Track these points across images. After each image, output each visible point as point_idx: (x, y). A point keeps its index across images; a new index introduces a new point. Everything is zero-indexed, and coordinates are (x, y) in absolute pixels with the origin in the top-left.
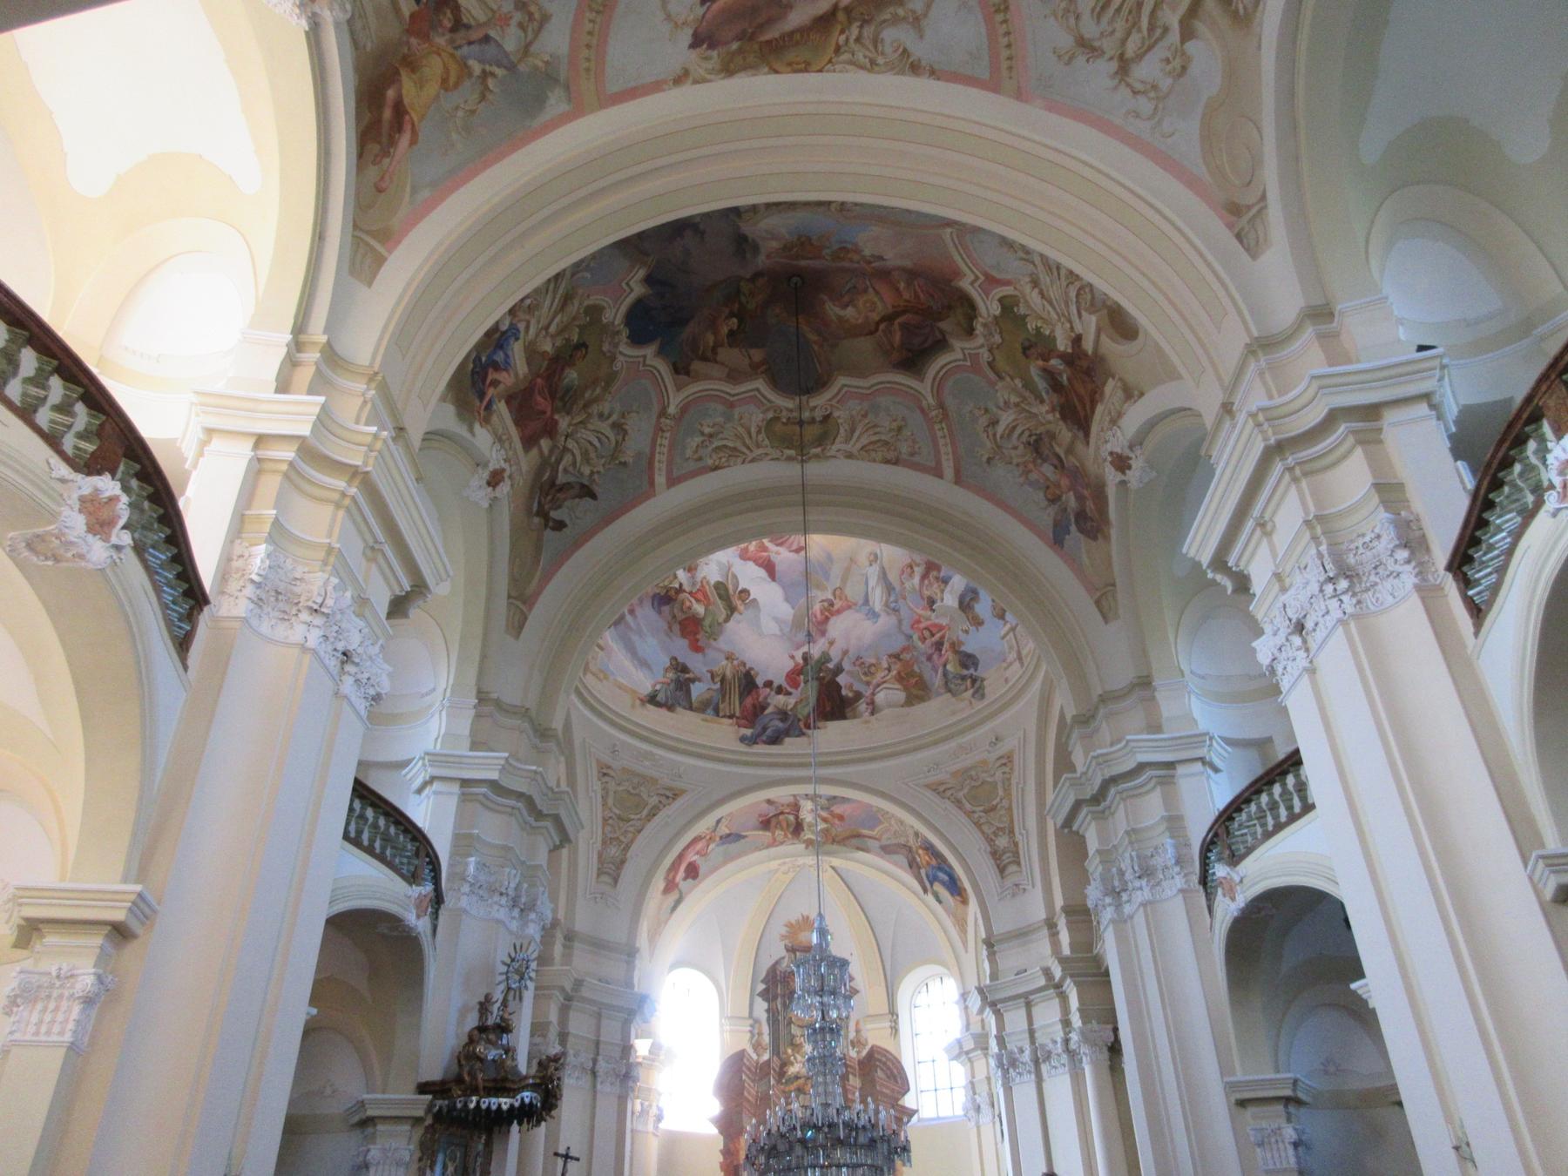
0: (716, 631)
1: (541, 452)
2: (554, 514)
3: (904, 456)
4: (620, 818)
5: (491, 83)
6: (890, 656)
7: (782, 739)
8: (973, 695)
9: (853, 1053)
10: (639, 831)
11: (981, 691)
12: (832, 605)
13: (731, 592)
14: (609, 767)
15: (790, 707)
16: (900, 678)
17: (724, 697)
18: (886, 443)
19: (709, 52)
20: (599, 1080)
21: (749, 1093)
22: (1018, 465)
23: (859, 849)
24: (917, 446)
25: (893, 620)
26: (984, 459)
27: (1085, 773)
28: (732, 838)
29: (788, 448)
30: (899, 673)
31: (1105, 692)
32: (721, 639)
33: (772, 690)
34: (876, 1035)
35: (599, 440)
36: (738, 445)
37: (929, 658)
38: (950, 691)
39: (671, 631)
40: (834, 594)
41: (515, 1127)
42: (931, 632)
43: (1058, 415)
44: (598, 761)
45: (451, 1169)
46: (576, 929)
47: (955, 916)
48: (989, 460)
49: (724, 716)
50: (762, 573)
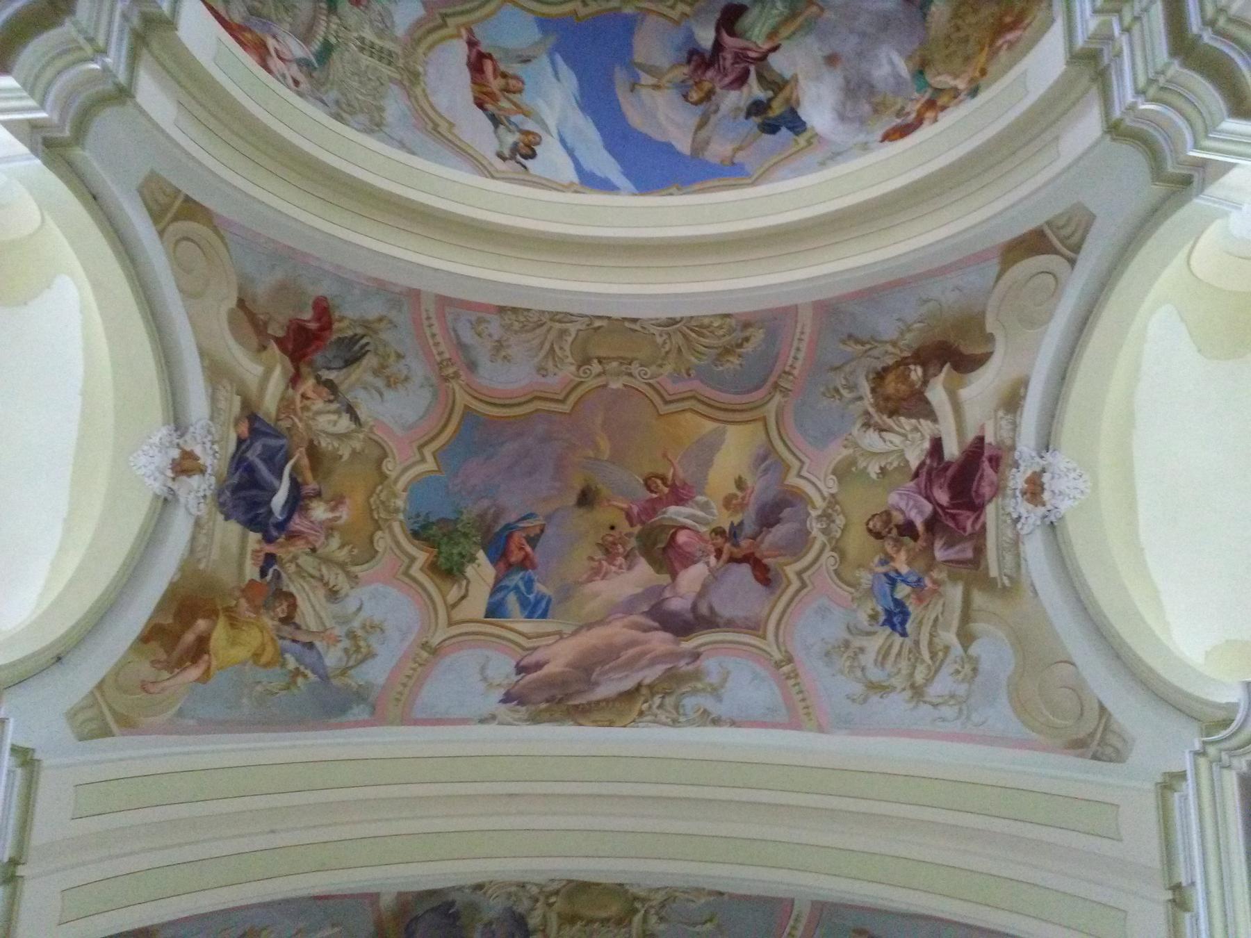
5: (300, 680)
19: (519, 707)
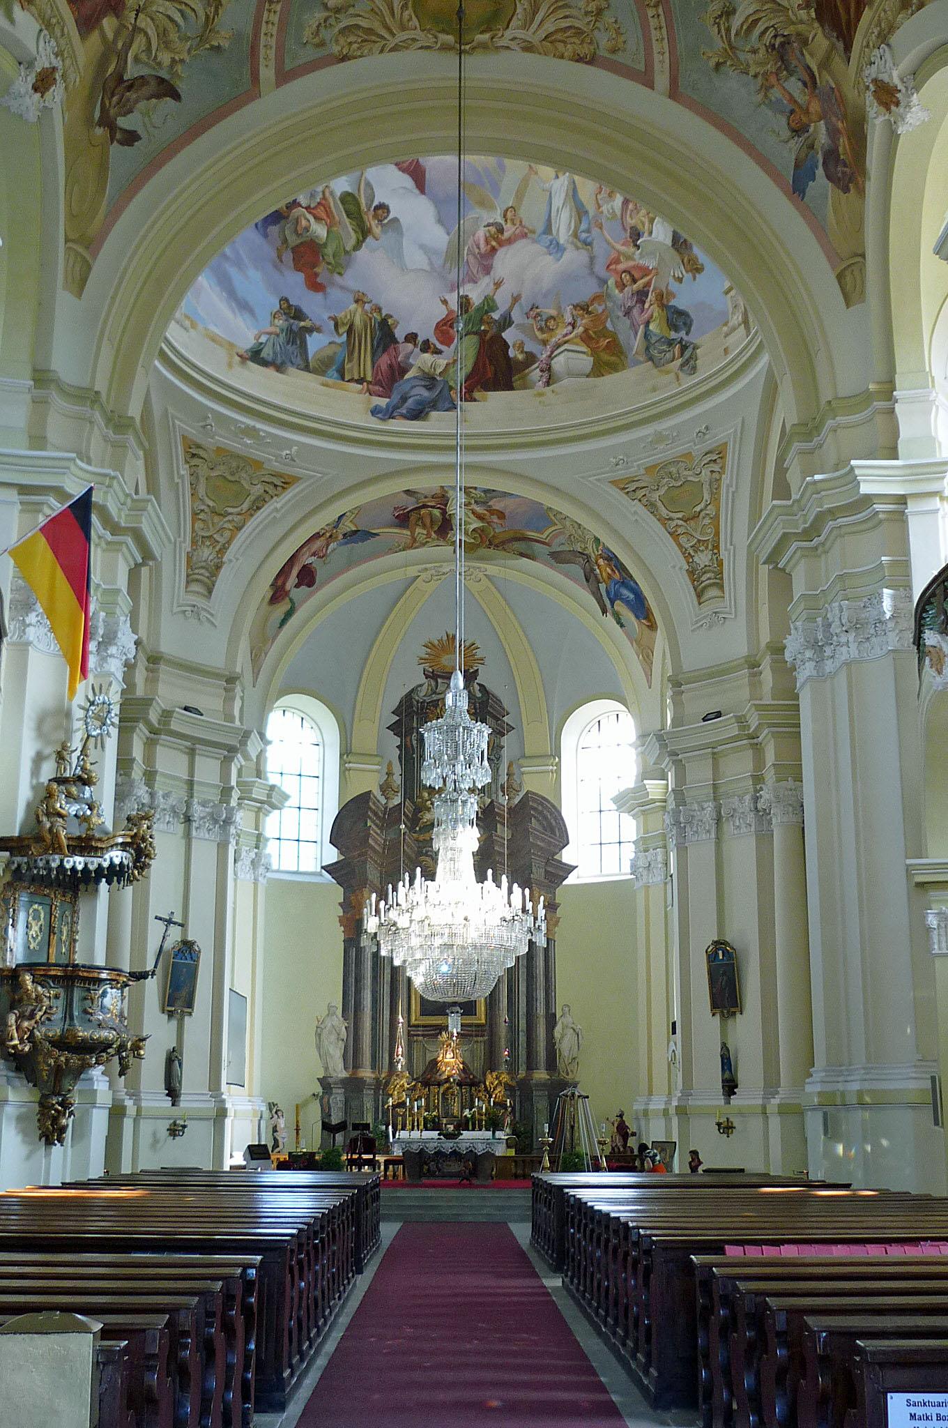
0: (341, 264)
1: (103, 36)
2: (122, 122)
3: (603, 53)
4: (214, 512)
6: (575, 307)
7: (427, 413)
8: (682, 365)
9: (504, 800)
10: (239, 529)
11: (692, 362)
12: (501, 230)
13: (364, 207)
14: (199, 446)
15: (438, 371)
16: (586, 338)
17: (351, 353)
18: (579, 32)
20: (195, 825)
21: (376, 841)
22: (755, 76)
23: (522, 555)
24: (622, 39)
25: (582, 256)
26: (712, 63)
27: (798, 501)
28: (356, 536)
29: (443, 31)
30: (586, 331)
31: (837, 398)
32: (349, 273)
33: (415, 345)
34: (531, 783)
35: (180, 11)
36: (377, 26)
37: (628, 313)
38: (651, 359)
39: (281, 261)
40: (505, 216)
41: (103, 885)
42: (632, 276)
43: (813, 15)
44: (184, 437)
45: (35, 928)
46: (162, 649)
47: (638, 643)
48: (718, 65)
49: (348, 381)
50: (407, 181)
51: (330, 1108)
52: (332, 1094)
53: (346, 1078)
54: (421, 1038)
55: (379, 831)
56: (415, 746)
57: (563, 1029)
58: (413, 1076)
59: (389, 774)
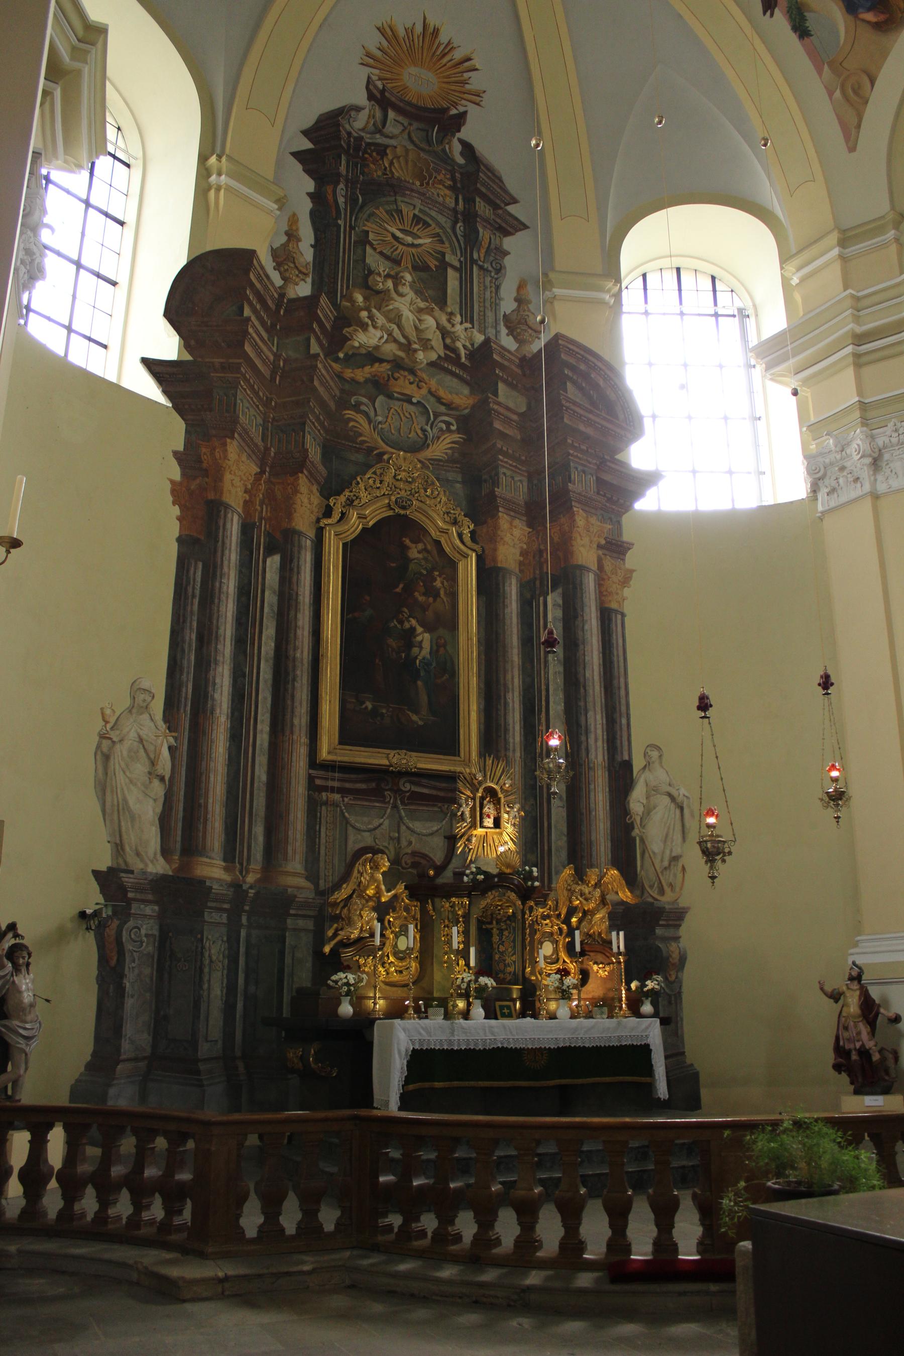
9: (508, 342)
51: (121, 952)
52: (129, 915)
53: (164, 877)
54: (337, 797)
55: (265, 335)
56: (342, 204)
57: (648, 797)
58: (317, 885)
59: (292, 235)
